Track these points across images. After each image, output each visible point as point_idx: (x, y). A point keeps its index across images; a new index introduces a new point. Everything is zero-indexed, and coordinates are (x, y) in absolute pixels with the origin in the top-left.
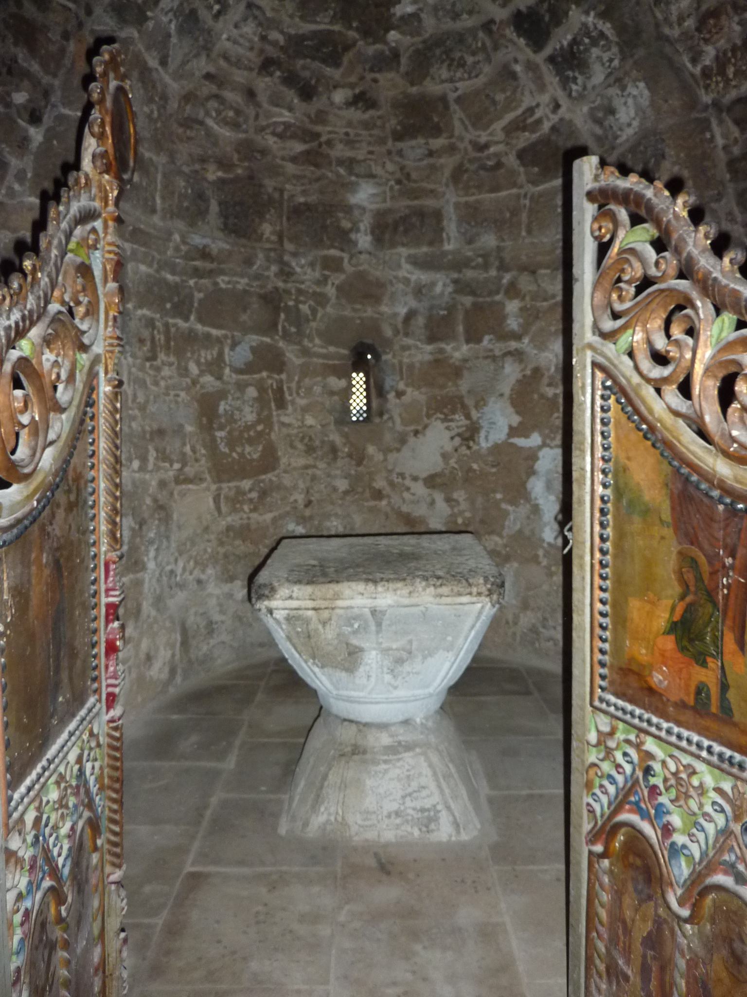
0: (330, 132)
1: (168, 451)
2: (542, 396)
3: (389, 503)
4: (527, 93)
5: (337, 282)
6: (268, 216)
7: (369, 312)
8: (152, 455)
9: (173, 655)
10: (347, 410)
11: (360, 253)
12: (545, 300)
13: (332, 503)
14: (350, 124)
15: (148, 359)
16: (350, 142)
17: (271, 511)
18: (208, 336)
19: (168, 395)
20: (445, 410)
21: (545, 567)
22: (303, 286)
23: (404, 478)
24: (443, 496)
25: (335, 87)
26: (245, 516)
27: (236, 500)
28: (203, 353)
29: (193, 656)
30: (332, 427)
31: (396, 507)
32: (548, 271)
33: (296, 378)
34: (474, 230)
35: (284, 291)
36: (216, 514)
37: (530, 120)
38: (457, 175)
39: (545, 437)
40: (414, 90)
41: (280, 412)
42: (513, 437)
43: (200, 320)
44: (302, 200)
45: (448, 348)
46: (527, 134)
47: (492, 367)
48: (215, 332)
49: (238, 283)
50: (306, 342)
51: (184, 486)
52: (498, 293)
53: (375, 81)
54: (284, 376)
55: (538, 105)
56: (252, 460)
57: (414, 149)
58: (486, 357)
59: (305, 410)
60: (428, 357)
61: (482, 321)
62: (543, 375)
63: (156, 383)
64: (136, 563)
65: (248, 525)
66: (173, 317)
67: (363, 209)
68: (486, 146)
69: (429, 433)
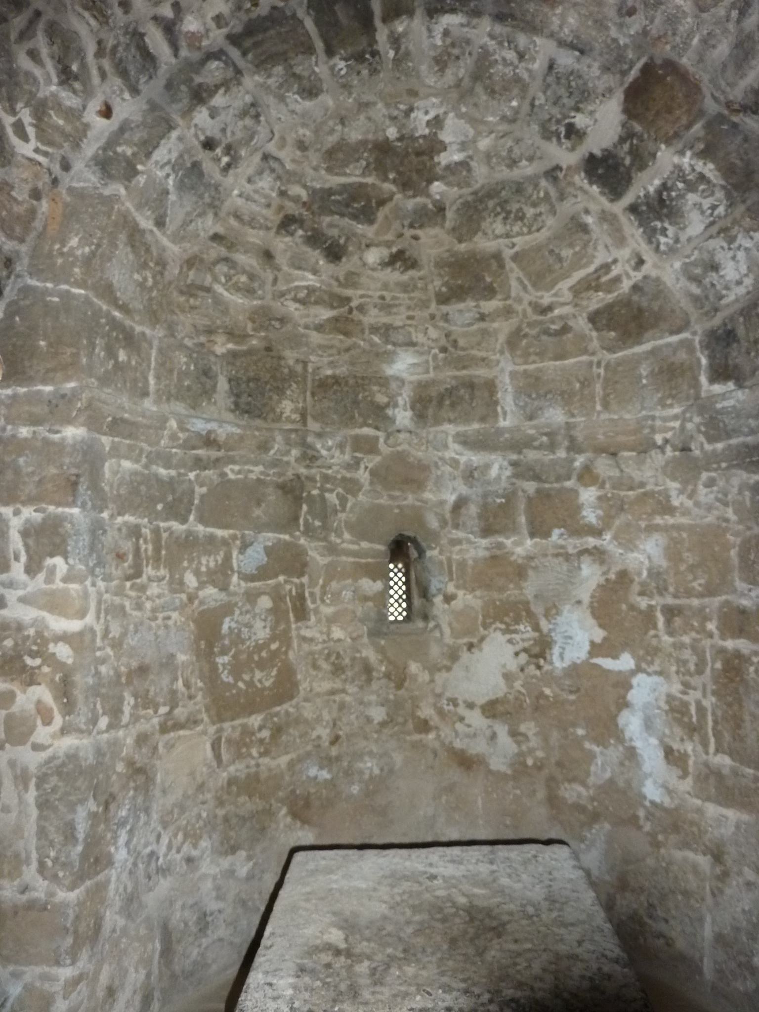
0: (362, 296)
1: (152, 693)
2: (632, 607)
3: (438, 736)
4: (600, 247)
5: (370, 465)
6: (288, 392)
7: (411, 499)
8: (129, 700)
9: (148, 975)
10: (382, 617)
11: (399, 431)
12: (631, 488)
13: (366, 738)
14: (385, 286)
15: (128, 578)
16: (386, 307)
17: (287, 753)
18: (211, 538)
19: (156, 618)
20: (507, 619)
21: (648, 834)
22: (330, 472)
23: (456, 705)
24: (506, 728)
25: (368, 246)
26: (253, 762)
27: (241, 744)
28: (204, 561)
29: (177, 968)
30: (365, 640)
31: (447, 742)
32: (634, 454)
33: (321, 582)
34: (536, 403)
35: (307, 478)
36: (215, 764)
37: (604, 279)
38: (514, 340)
39: (639, 660)
40: (463, 247)
41: (299, 624)
42: (597, 656)
43: (201, 520)
44: (329, 372)
45: (508, 542)
46: (600, 294)
47: (565, 568)
48: (220, 533)
49: (252, 472)
50: (333, 537)
51: (172, 734)
52: (569, 479)
53: (416, 238)
54: (305, 580)
55: (615, 261)
56: (264, 689)
57: (463, 312)
58: (557, 555)
59: (331, 620)
60: (482, 553)
61: (549, 511)
62: (632, 581)
63: (139, 607)
64: (97, 860)
65: (257, 774)
66: (167, 520)
67: (403, 382)
68: (550, 308)
69: (485, 646)
